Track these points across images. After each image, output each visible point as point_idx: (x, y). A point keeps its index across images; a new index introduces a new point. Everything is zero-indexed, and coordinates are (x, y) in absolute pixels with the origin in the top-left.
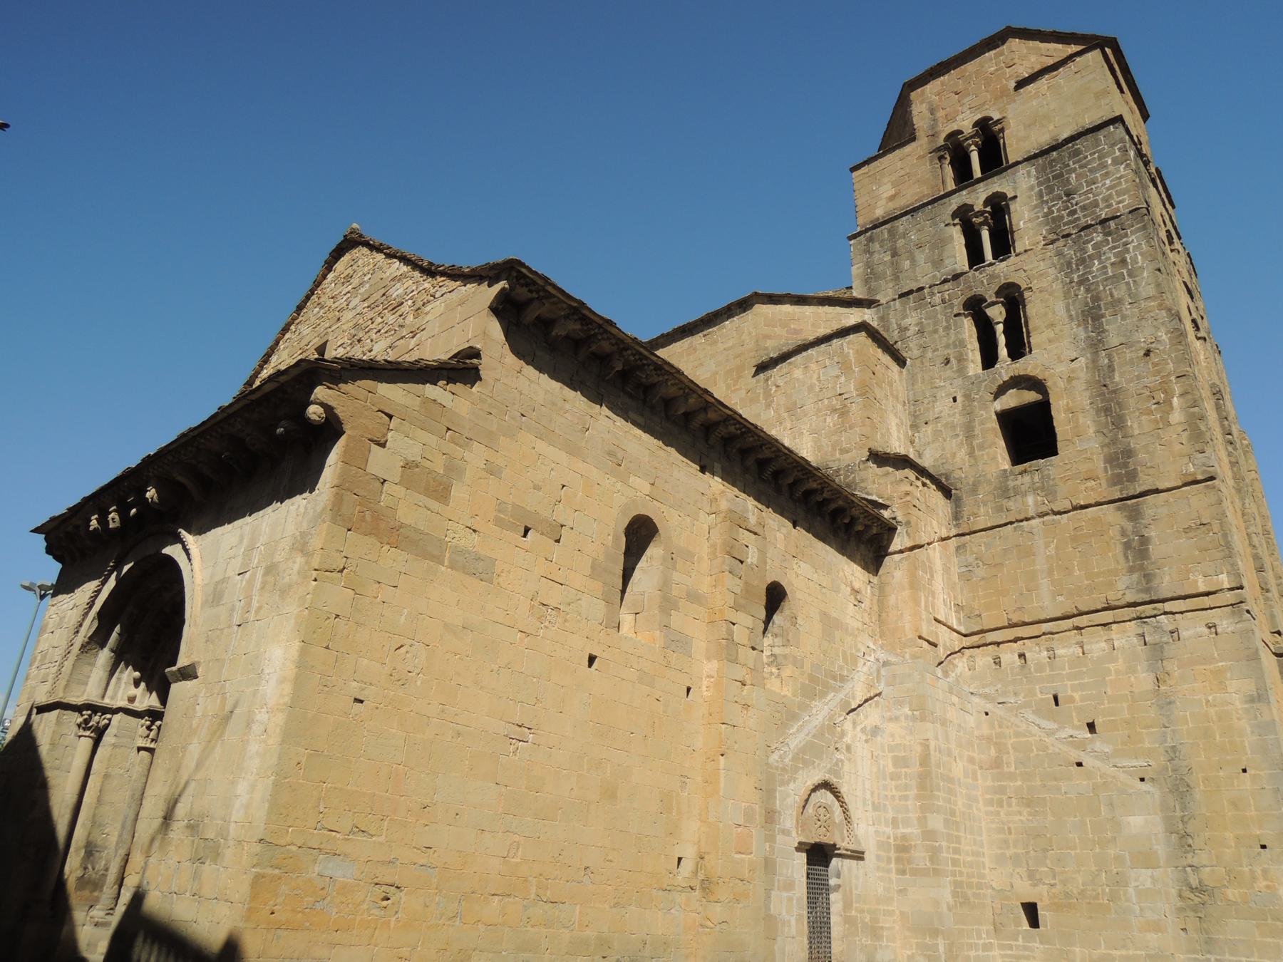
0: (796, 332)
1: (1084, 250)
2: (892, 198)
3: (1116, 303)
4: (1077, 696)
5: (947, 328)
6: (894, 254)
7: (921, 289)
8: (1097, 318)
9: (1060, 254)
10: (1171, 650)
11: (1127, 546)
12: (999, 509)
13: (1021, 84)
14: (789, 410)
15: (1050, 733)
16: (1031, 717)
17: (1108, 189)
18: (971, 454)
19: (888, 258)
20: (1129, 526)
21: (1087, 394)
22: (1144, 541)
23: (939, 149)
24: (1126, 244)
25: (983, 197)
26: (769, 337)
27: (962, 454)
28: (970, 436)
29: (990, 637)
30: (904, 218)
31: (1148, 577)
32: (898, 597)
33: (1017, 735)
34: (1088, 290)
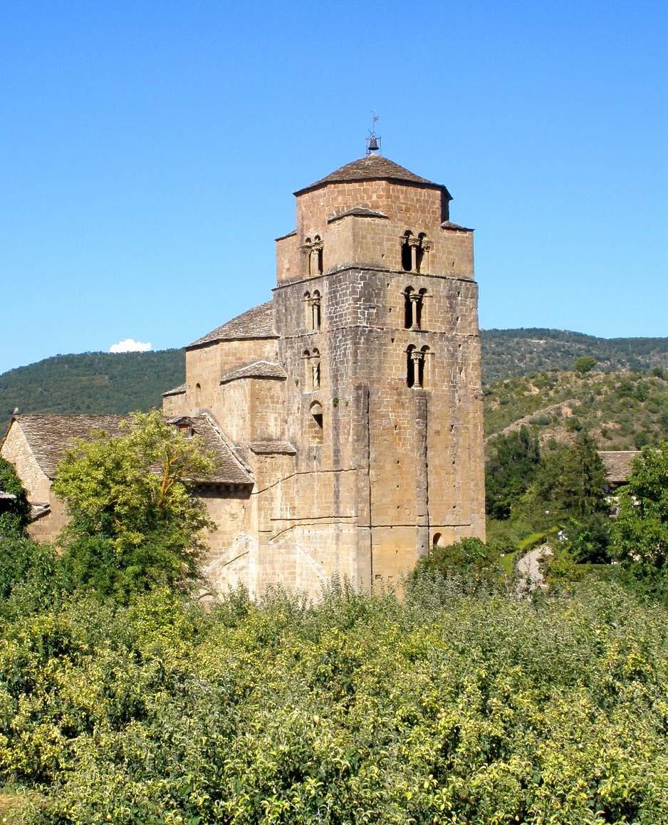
0: (240, 359)
1: (336, 341)
2: (288, 269)
3: (342, 375)
4: (320, 550)
5: (298, 365)
6: (286, 310)
7: (291, 338)
8: (337, 380)
9: (330, 339)
10: (340, 537)
11: (335, 491)
12: (307, 465)
13: (330, 222)
14: (230, 411)
15: (313, 564)
16: (310, 558)
17: (347, 309)
18: (302, 435)
19: (284, 311)
20: (336, 483)
21: (331, 418)
22: (339, 491)
23: (303, 247)
24: (347, 345)
25: (313, 291)
26: (227, 363)
27: (300, 433)
28: (302, 427)
29: (303, 522)
30: (290, 288)
31: (338, 507)
32: (254, 513)
33: (307, 564)
34: (336, 365)
